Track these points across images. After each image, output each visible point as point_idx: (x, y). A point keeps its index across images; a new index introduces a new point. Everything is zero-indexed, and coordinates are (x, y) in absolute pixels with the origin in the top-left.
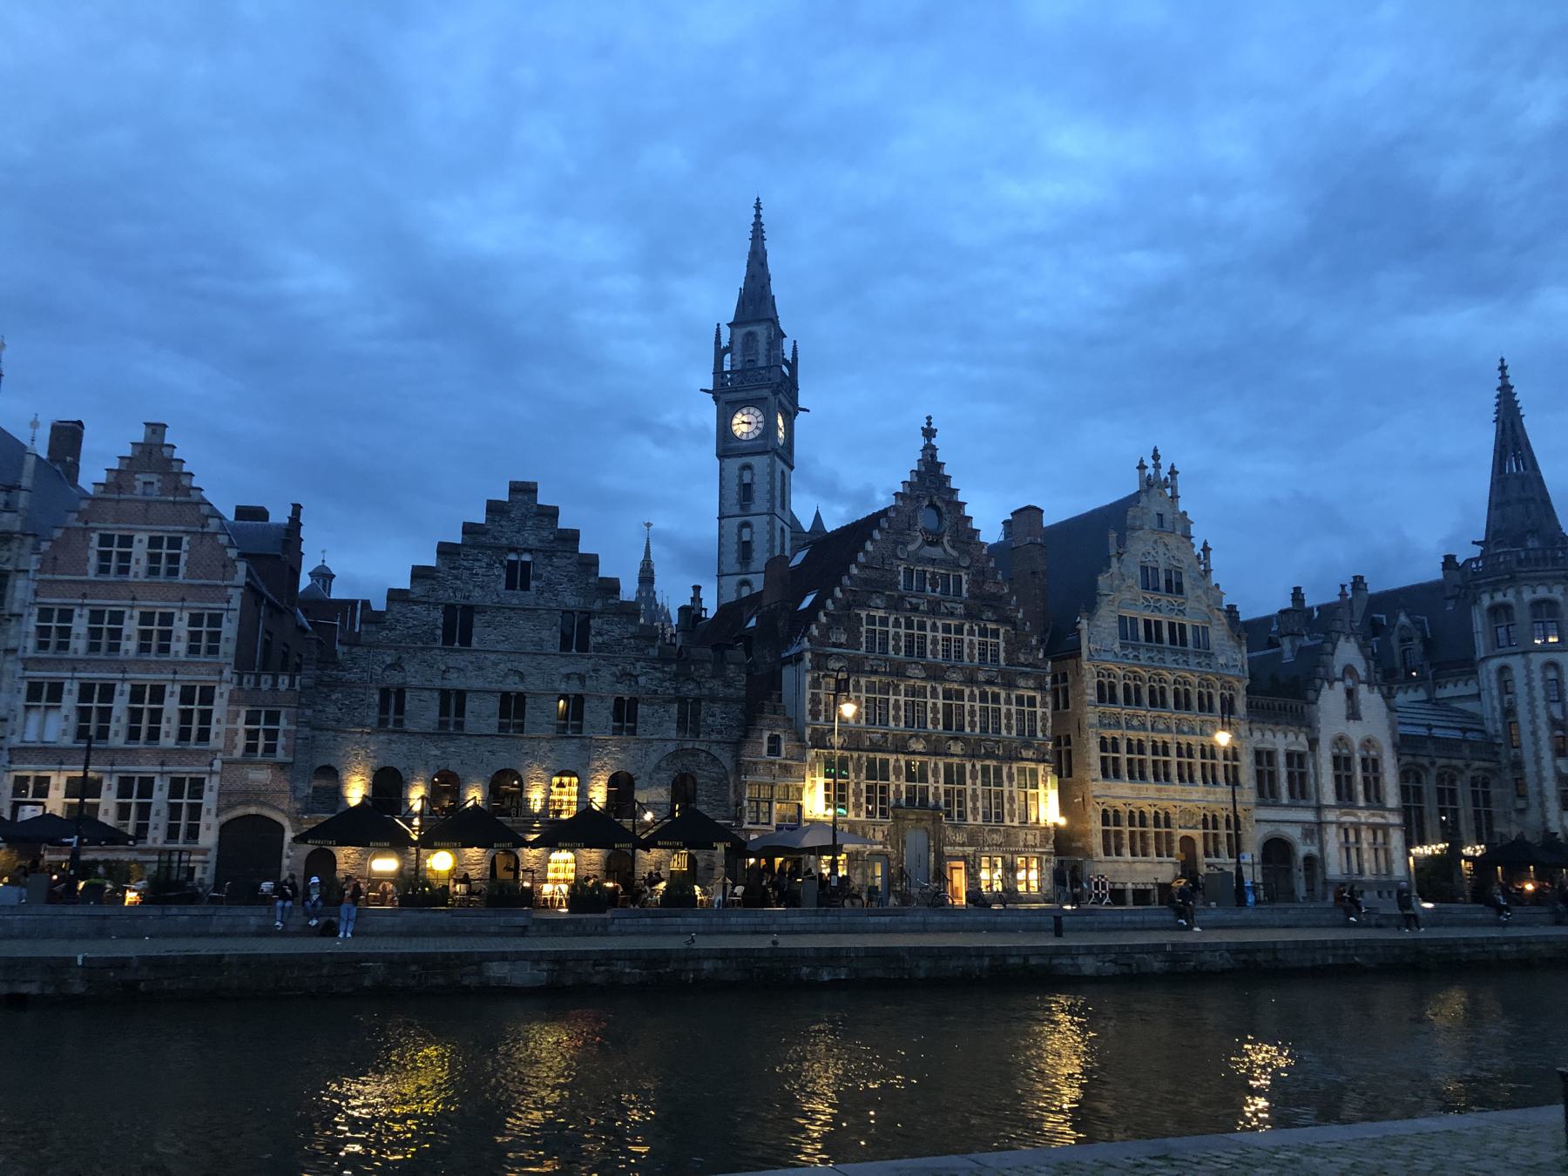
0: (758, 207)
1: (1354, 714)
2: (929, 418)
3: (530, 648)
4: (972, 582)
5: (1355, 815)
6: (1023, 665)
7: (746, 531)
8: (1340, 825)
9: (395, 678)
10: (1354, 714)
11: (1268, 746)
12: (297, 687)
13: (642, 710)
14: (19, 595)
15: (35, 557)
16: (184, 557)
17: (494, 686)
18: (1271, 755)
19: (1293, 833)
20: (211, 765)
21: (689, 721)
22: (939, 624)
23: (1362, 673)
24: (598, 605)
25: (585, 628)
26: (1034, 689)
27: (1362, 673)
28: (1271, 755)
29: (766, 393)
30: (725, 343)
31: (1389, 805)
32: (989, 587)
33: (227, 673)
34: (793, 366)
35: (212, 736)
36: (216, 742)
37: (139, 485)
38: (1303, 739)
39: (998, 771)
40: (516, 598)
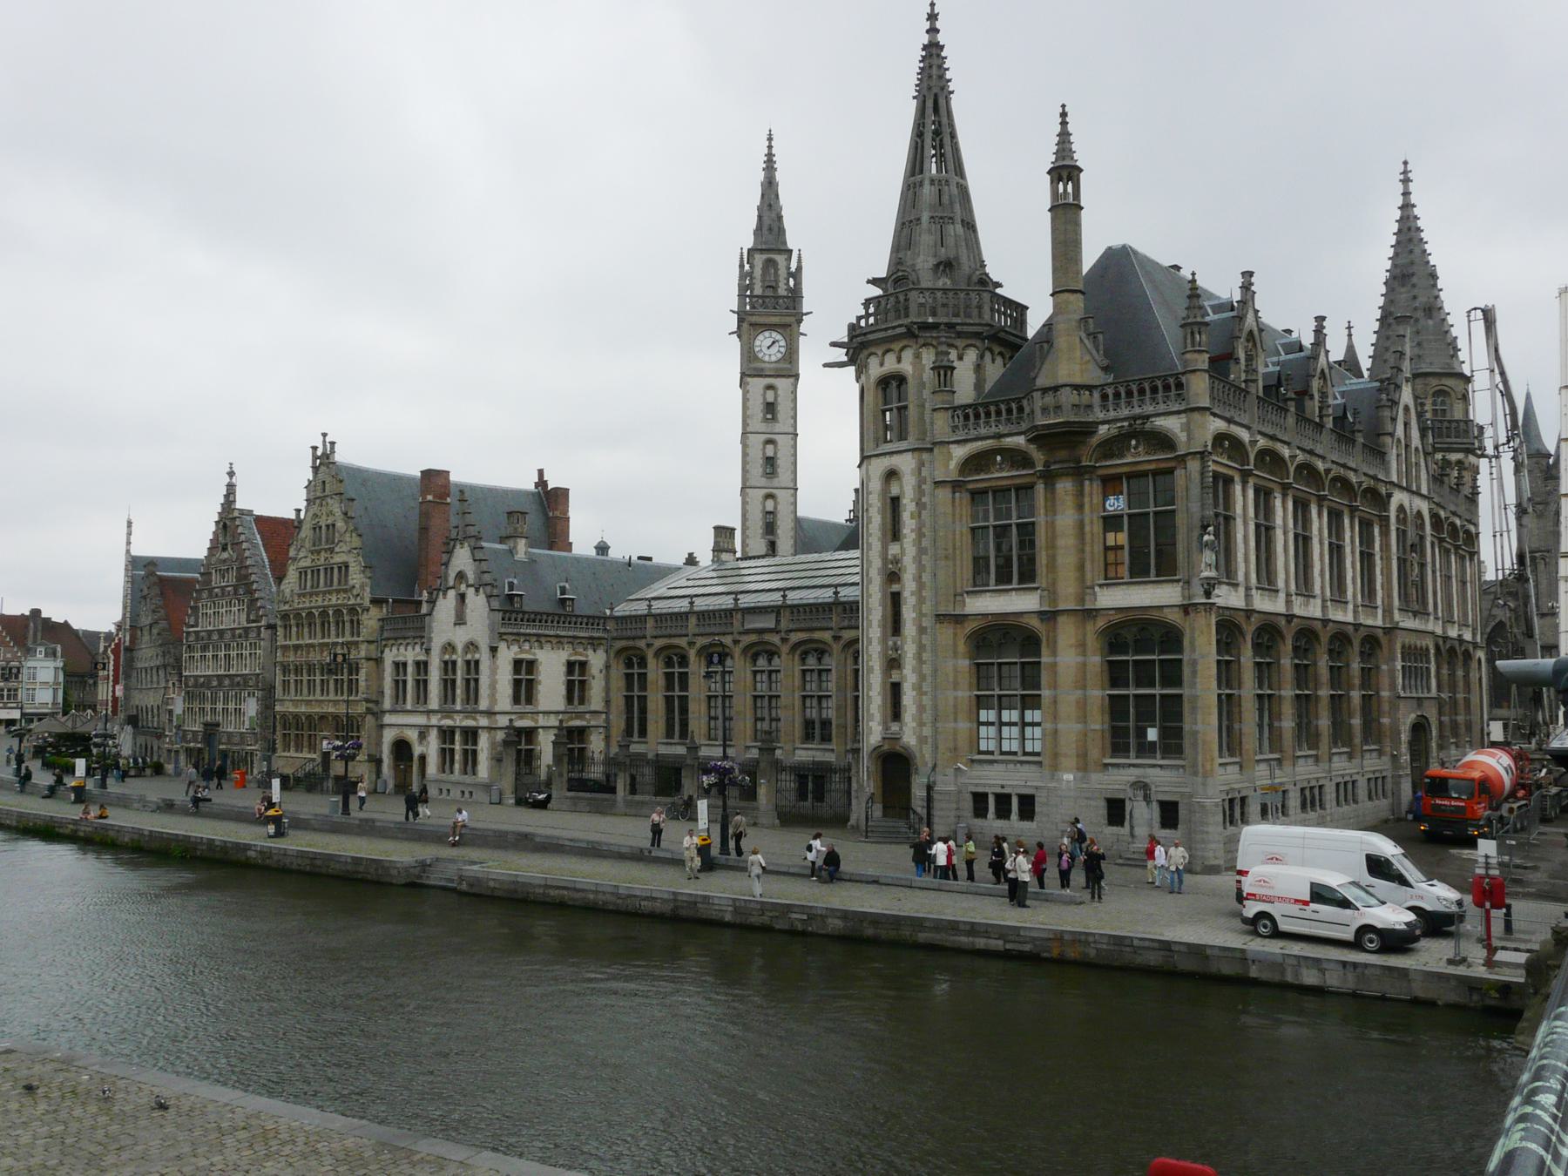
0: (770, 139)
1: (460, 620)
7: (770, 448)
8: (440, 728)
10: (460, 620)
11: (401, 659)
18: (405, 664)
19: (412, 735)
34: (797, 275)
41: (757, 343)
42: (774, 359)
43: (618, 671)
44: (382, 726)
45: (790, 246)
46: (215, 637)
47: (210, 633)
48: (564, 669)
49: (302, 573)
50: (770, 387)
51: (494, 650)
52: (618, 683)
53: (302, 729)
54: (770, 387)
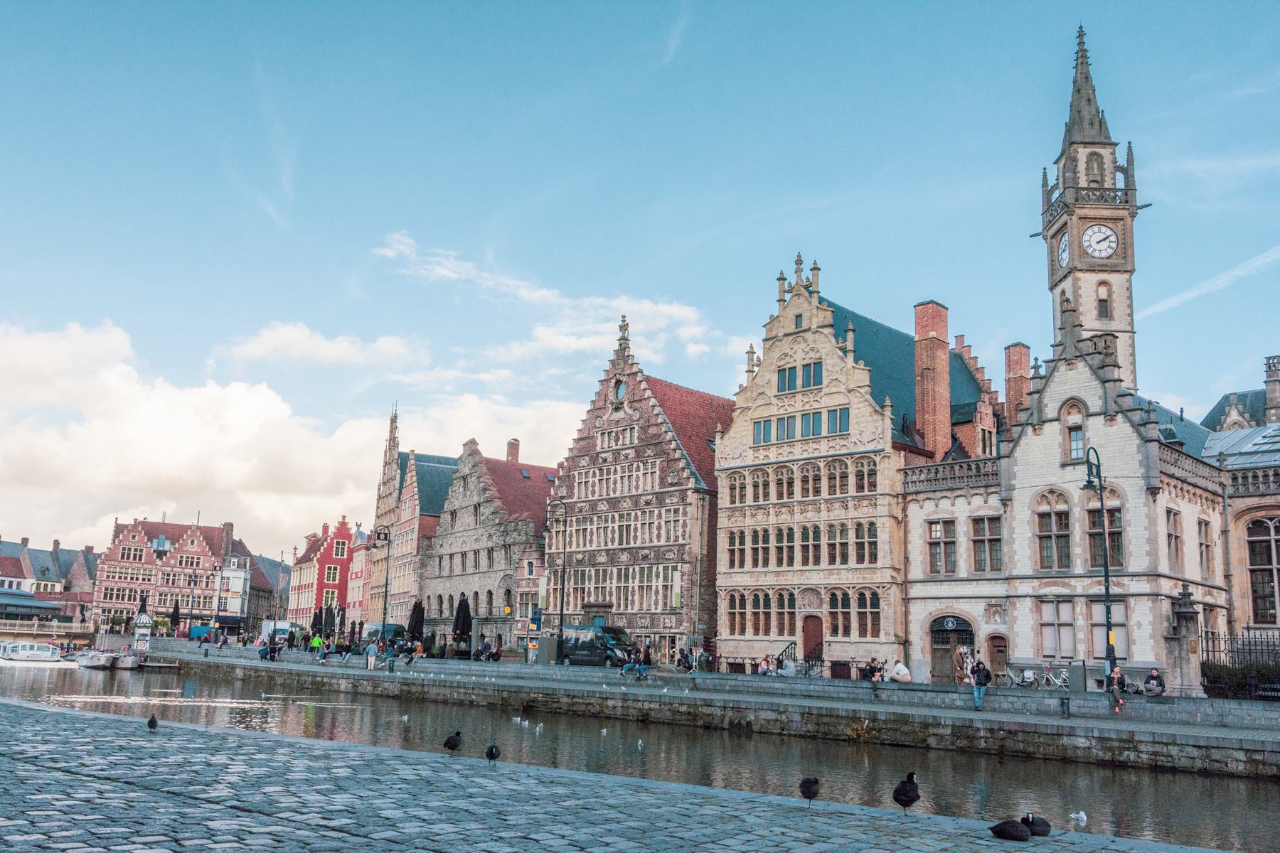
2: (624, 317)
4: (642, 428)
5: (1065, 585)
6: (672, 485)
8: (1041, 600)
18: (949, 524)
21: (509, 560)
22: (618, 468)
23: (1095, 404)
26: (678, 504)
27: (1095, 404)
28: (949, 524)
29: (1065, 217)
30: (1051, 182)
31: (1131, 569)
32: (652, 430)
34: (1127, 171)
38: (994, 500)
39: (650, 569)
41: (1086, 238)
42: (1104, 254)
43: (1239, 534)
44: (906, 600)
45: (1114, 140)
46: (603, 507)
47: (593, 505)
48: (1197, 528)
49: (761, 426)
50: (1103, 283)
51: (1153, 491)
52: (1240, 554)
53: (764, 609)
54: (1103, 283)
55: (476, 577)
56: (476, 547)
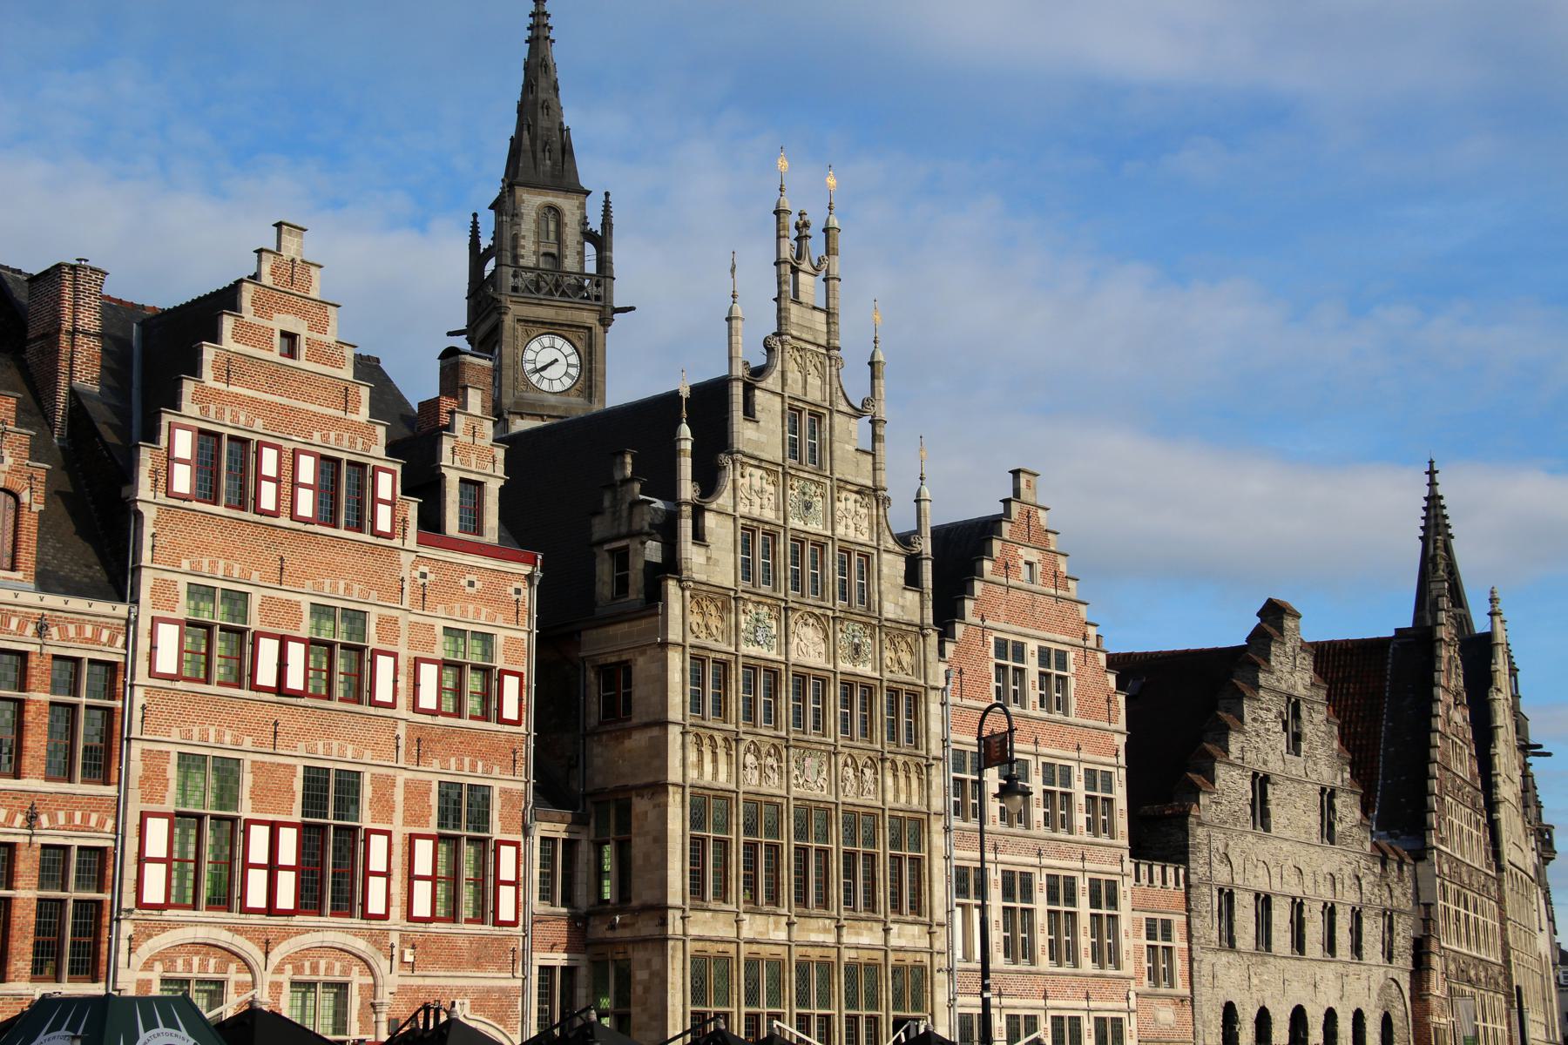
3: (1303, 838)
9: (1222, 875)
12: (1182, 885)
13: (1367, 925)
14: (935, 727)
15: (943, 667)
16: (1072, 683)
17: (1287, 890)
20: (1128, 999)
24: (1338, 782)
25: (1332, 808)
33: (1127, 858)
35: (1123, 956)
36: (1128, 968)
37: (1021, 563)
40: (1296, 766)
55: (1329, 971)
56: (1327, 895)
